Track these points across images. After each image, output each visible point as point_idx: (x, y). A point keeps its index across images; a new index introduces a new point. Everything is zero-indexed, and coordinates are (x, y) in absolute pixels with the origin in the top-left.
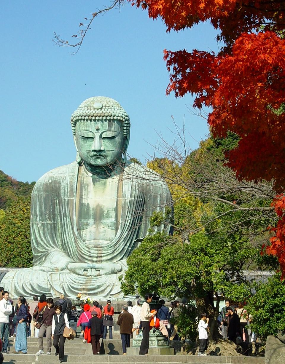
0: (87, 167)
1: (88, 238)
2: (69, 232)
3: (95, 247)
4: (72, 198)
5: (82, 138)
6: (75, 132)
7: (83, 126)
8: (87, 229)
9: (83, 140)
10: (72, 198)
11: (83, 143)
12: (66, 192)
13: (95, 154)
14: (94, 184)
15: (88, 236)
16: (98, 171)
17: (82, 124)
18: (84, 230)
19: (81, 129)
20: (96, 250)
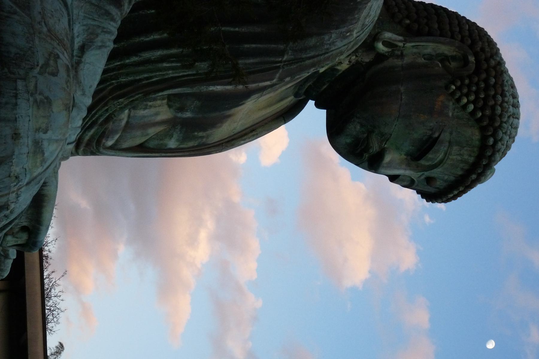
0: (350, 62)
1: (141, 113)
2: (174, 64)
3: (104, 133)
4: (278, 75)
5: (430, 137)
6: (458, 100)
7: (459, 158)
8: (166, 106)
9: (424, 139)
10: (278, 75)
11: (416, 136)
12: (304, 56)
13: (371, 151)
14: (292, 86)
15: (146, 111)
16: (325, 87)
17: (466, 157)
18: (165, 101)
19: (455, 148)
20: (92, 137)
